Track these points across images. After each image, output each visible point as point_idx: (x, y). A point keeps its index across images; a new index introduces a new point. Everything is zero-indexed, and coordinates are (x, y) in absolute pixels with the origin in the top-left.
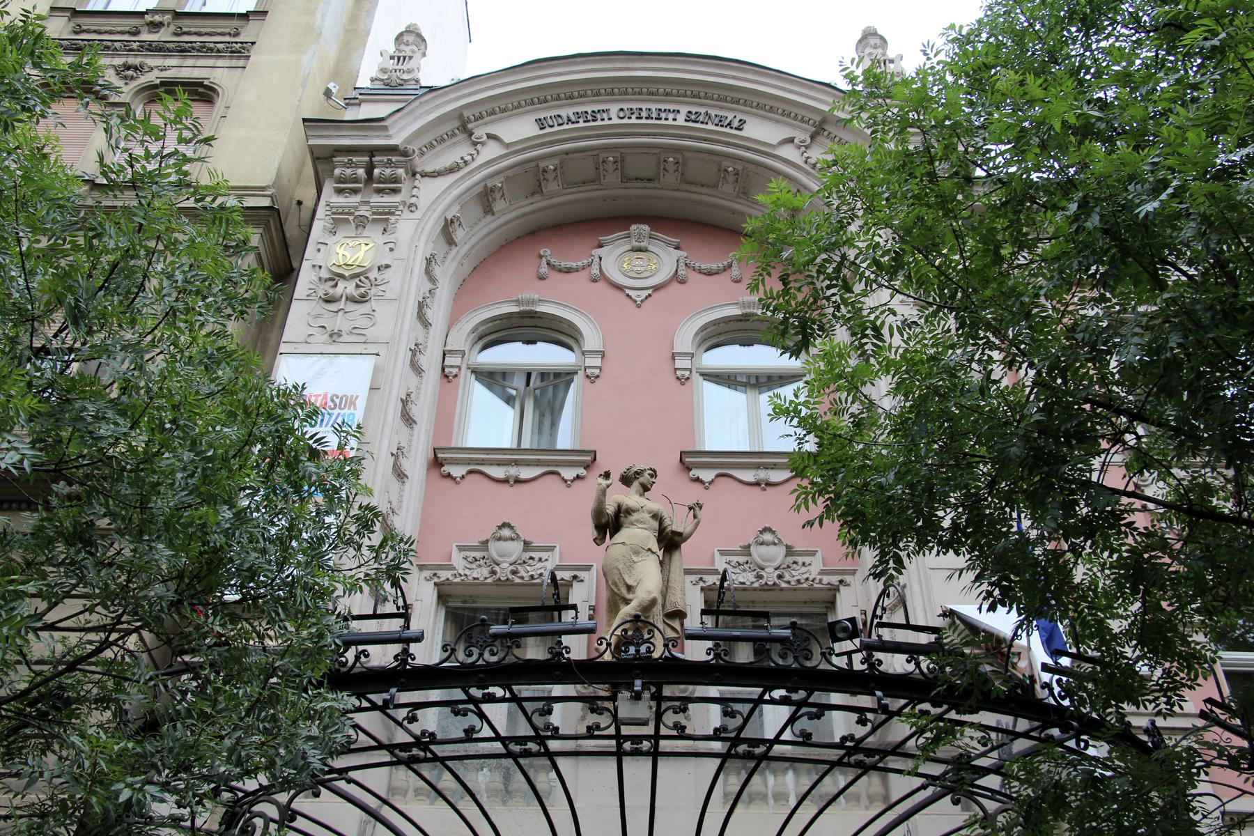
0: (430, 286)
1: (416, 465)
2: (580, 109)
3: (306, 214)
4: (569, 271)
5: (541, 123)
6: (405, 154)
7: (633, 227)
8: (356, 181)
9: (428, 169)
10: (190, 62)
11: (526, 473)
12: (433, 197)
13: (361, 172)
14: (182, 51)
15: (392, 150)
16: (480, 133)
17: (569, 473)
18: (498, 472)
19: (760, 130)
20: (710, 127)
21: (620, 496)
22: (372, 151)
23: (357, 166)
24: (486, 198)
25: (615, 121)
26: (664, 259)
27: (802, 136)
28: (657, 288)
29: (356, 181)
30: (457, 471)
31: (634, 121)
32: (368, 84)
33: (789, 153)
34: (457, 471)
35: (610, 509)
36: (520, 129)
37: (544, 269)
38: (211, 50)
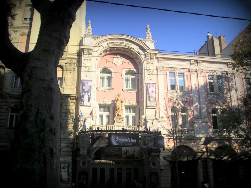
5: (108, 44)
6: (92, 50)
11: (106, 90)
12: (96, 54)
15: (90, 49)
16: (100, 45)
17: (111, 91)
20: (127, 45)
21: (117, 97)
22: (88, 49)
24: (101, 54)
30: (99, 90)
31: (119, 44)
33: (137, 50)
34: (99, 90)
37: (107, 62)
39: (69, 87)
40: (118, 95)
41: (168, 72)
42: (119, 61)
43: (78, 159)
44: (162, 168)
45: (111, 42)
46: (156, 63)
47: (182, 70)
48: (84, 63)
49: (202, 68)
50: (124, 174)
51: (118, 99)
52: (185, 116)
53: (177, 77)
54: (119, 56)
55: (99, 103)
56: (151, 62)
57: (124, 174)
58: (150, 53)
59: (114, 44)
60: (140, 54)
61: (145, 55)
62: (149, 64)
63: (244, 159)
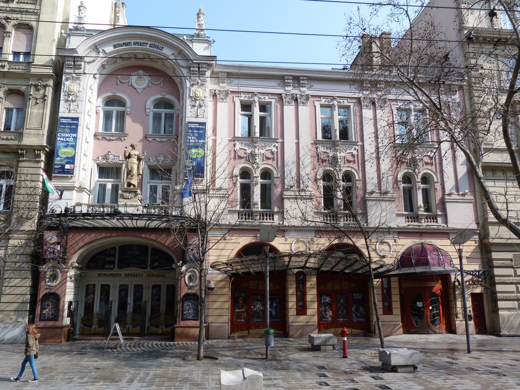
0: (91, 91)
1: (91, 139)
2: (124, 42)
3: (61, 65)
4: (124, 83)
7: (139, 71)
8: (71, 65)
9: (88, 61)
10: (24, 16)
13: (72, 63)
14: (20, 11)
18: (108, 138)
19: (167, 52)
22: (74, 57)
23: (71, 61)
24: (103, 66)
25: (133, 46)
26: (146, 80)
27: (176, 54)
28: (144, 89)
29: (71, 65)
32: (72, 28)
35: (127, 154)
36: (109, 49)
37: (119, 83)
38: (29, 12)
39: (33, 132)
40: (132, 146)
41: (317, 104)
42: (140, 82)
43: (43, 268)
44: (212, 285)
45: (121, 42)
46: (210, 85)
47: (267, 97)
48: (67, 85)
49: (307, 92)
50: (147, 296)
51: (131, 153)
52: (350, 188)
53: (336, 113)
54: (141, 72)
55: (149, 163)
56: (199, 81)
57: (147, 296)
58: (199, 64)
59: (128, 47)
60: (179, 65)
61: (189, 68)
62: (195, 87)
63: (357, 272)
